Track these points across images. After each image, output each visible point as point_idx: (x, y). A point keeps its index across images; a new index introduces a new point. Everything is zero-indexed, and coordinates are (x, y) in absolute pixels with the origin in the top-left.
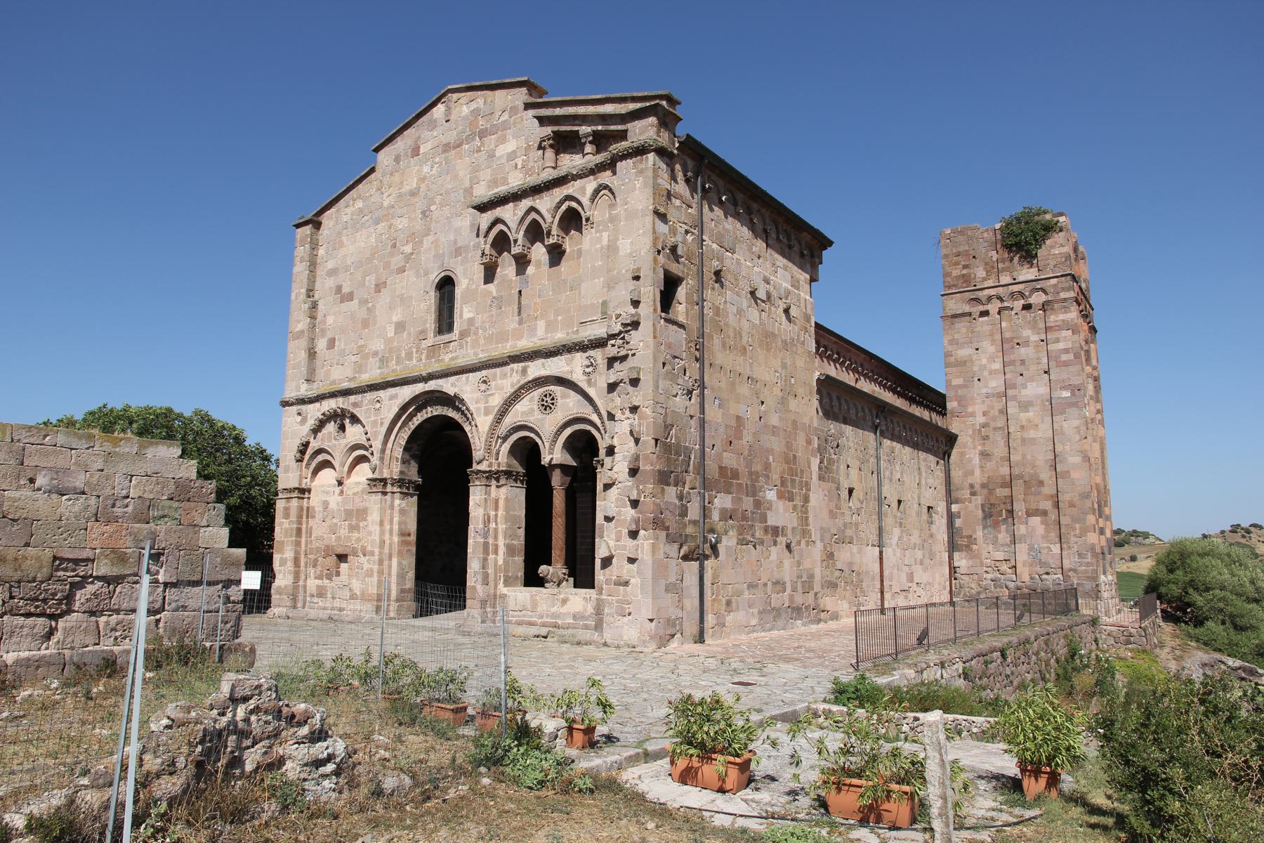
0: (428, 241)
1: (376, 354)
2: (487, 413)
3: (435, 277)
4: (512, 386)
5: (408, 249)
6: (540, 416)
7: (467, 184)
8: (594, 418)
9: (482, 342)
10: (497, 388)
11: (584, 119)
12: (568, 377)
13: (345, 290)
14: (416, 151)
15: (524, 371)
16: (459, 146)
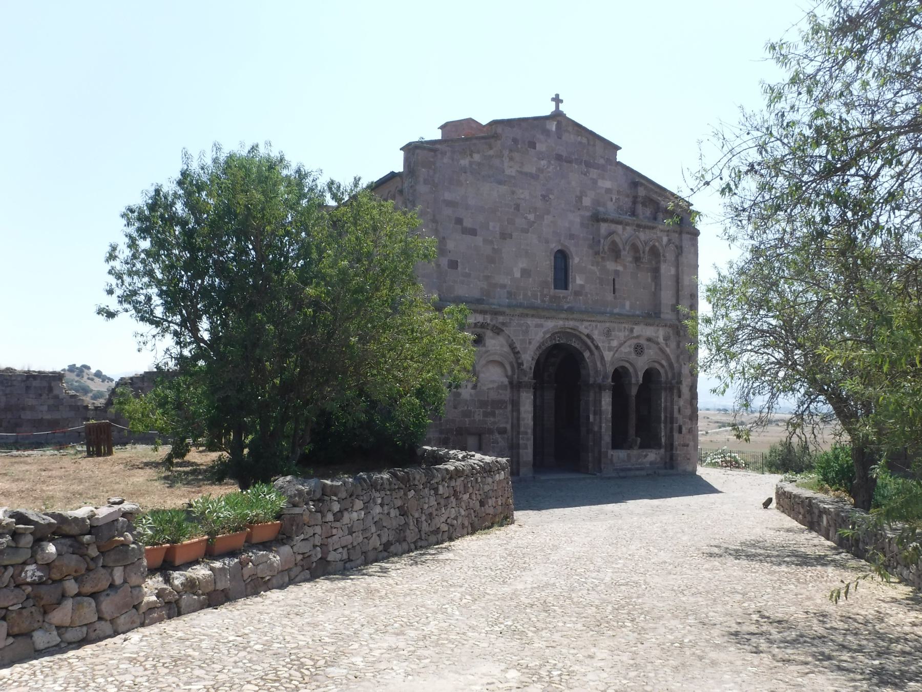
0: (548, 219)
1: (503, 286)
2: (610, 349)
3: (555, 247)
5: (531, 217)
7: (578, 194)
8: (664, 363)
13: (468, 223)
14: (532, 145)
15: (632, 330)
16: (570, 162)
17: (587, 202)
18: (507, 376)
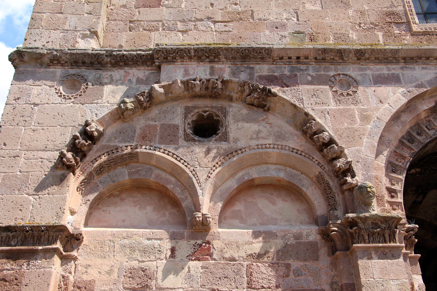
18: (316, 221)
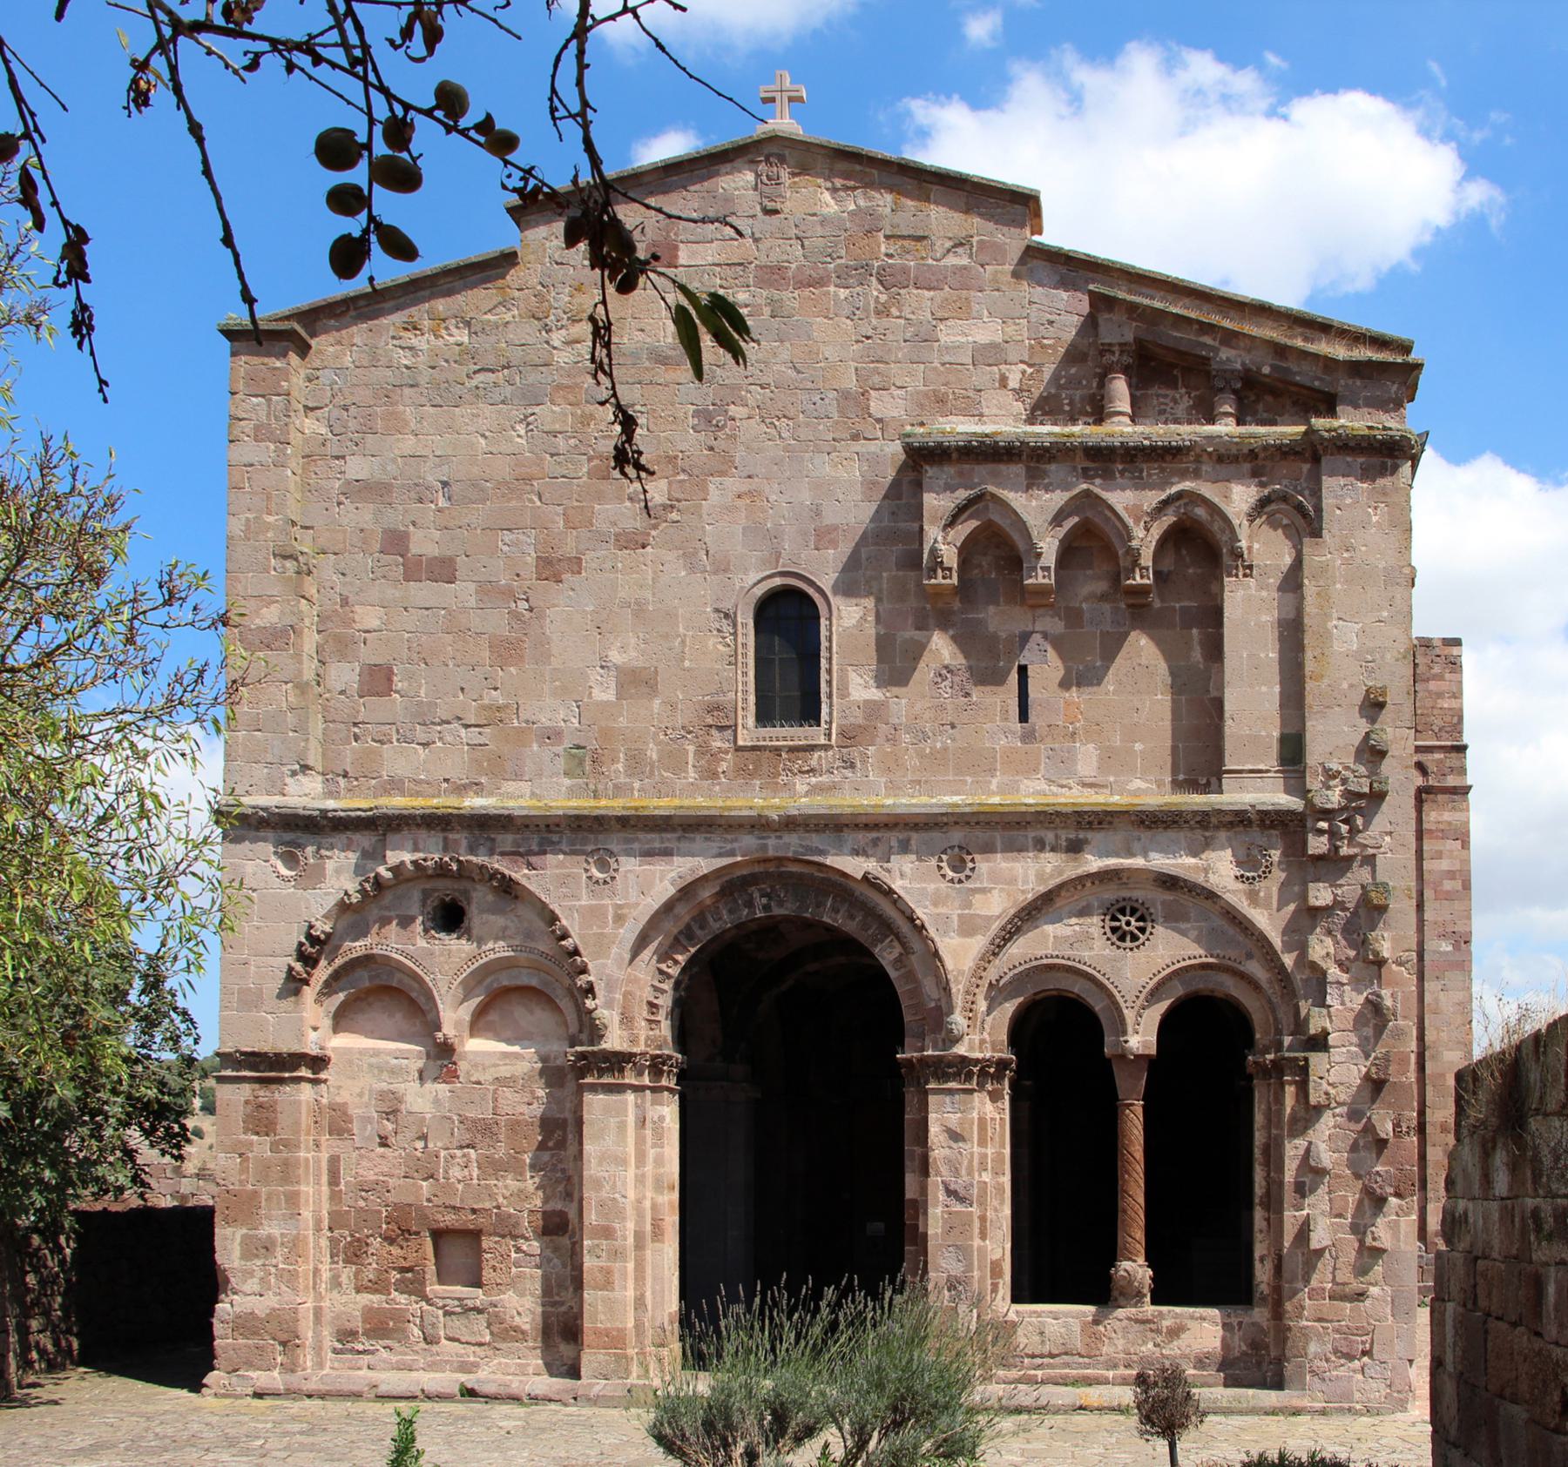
1: (551, 736)
2: (968, 927)
4: (1040, 877)
6: (1109, 951)
8: (1256, 969)
9: (911, 760)
10: (995, 877)
11: (1230, 337)
12: (1200, 880)
16: (820, 282)
17: (887, 406)
